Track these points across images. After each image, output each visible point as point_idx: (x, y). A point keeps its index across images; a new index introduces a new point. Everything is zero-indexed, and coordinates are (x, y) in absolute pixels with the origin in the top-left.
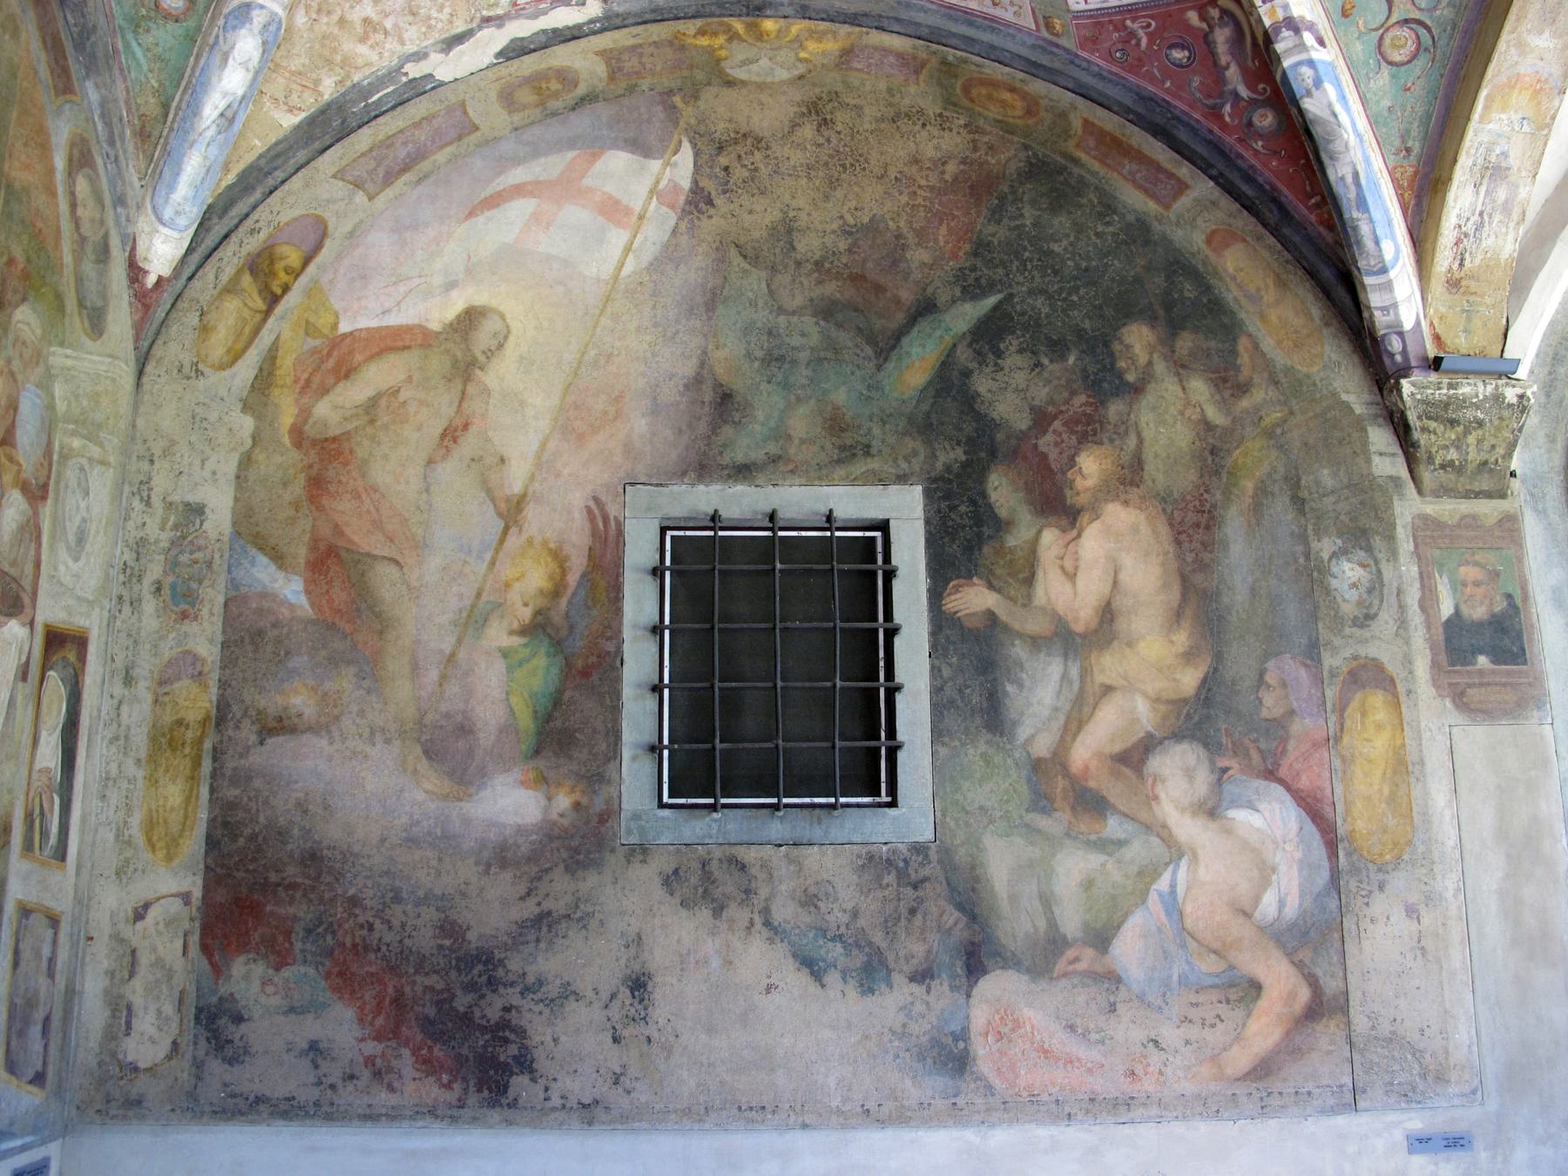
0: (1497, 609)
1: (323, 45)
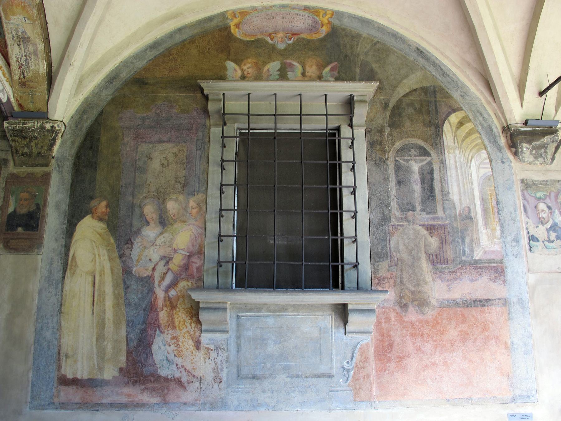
0: (31, 210)
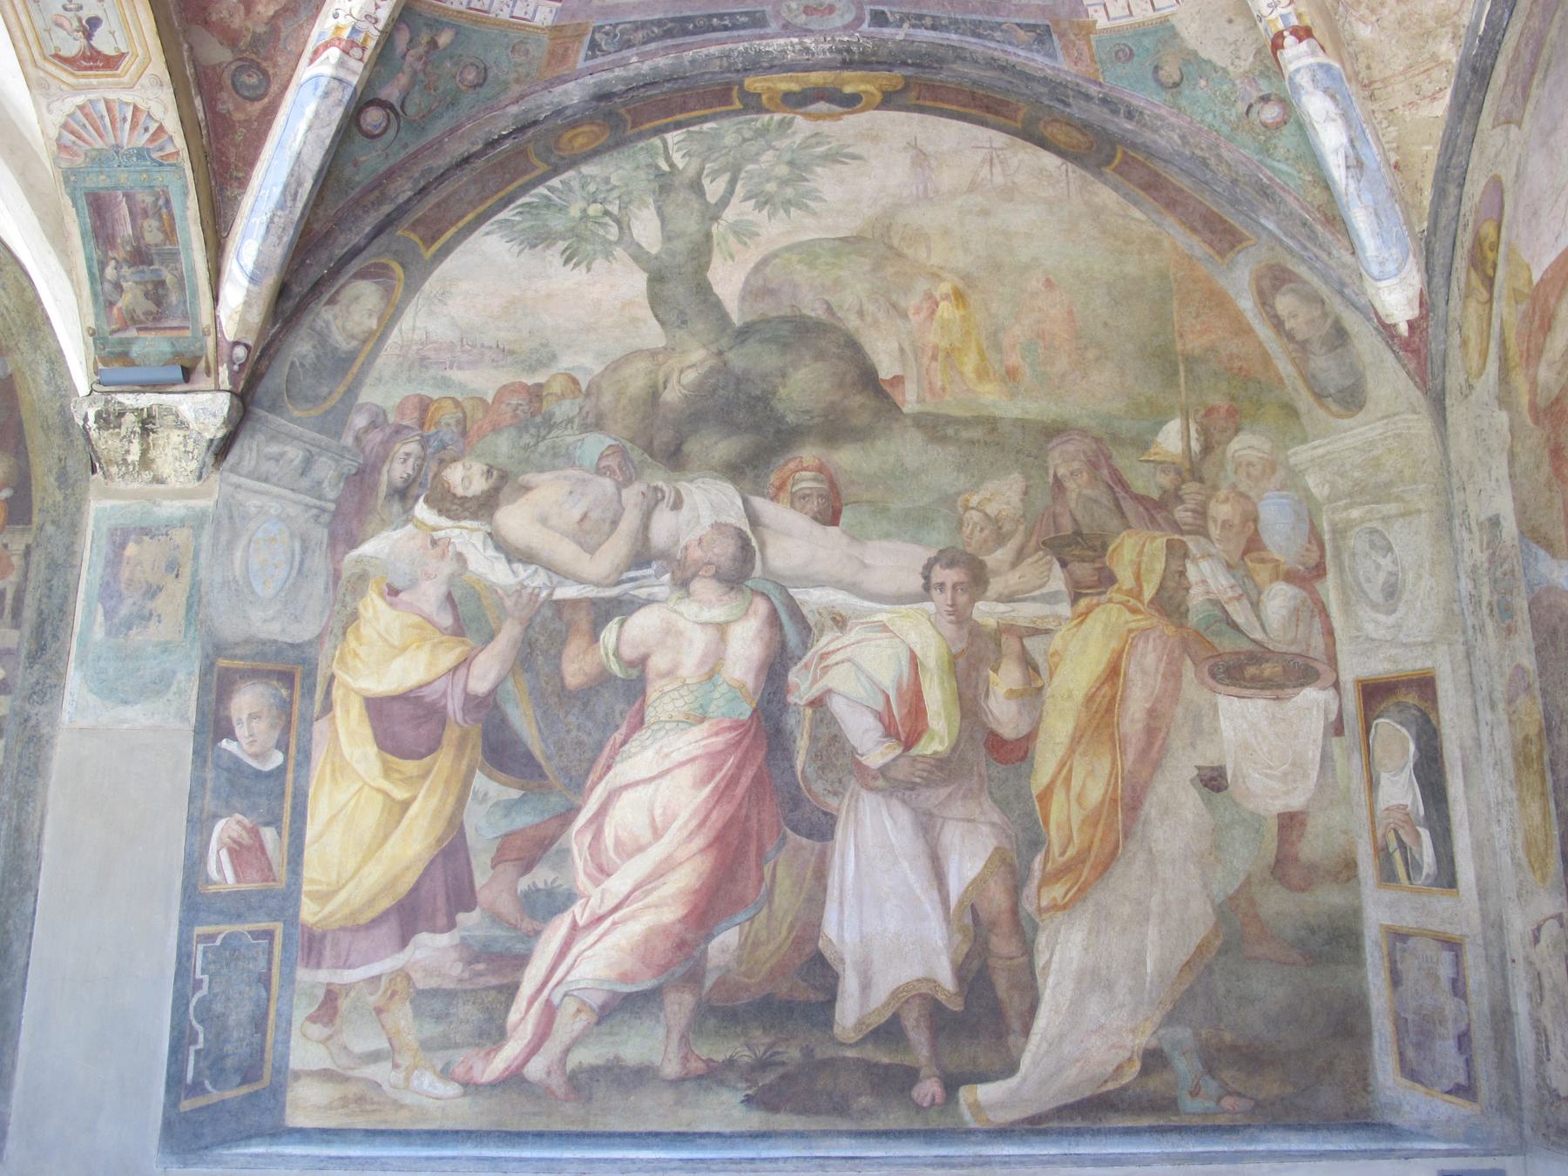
1: (1407, 29)
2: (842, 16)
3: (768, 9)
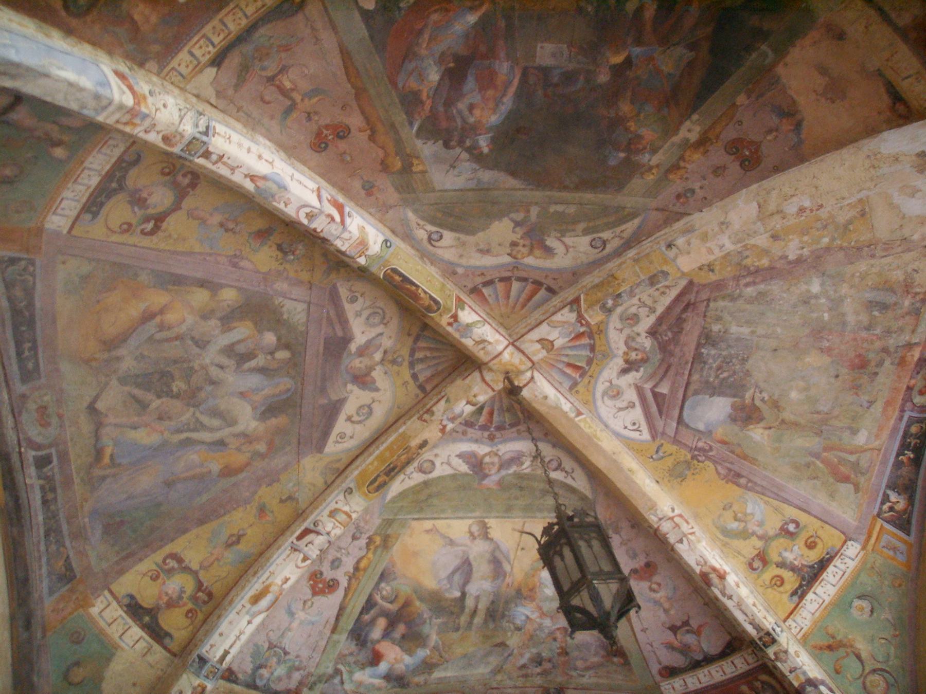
2: (40, 434)
3: (43, 381)
